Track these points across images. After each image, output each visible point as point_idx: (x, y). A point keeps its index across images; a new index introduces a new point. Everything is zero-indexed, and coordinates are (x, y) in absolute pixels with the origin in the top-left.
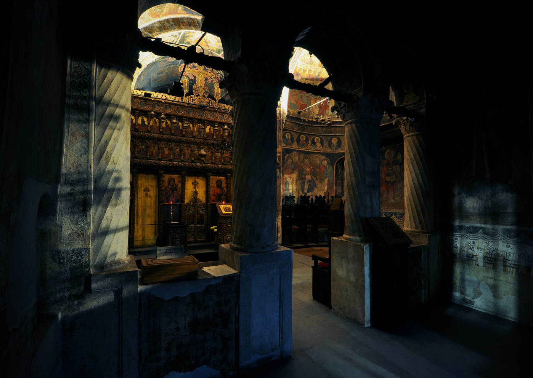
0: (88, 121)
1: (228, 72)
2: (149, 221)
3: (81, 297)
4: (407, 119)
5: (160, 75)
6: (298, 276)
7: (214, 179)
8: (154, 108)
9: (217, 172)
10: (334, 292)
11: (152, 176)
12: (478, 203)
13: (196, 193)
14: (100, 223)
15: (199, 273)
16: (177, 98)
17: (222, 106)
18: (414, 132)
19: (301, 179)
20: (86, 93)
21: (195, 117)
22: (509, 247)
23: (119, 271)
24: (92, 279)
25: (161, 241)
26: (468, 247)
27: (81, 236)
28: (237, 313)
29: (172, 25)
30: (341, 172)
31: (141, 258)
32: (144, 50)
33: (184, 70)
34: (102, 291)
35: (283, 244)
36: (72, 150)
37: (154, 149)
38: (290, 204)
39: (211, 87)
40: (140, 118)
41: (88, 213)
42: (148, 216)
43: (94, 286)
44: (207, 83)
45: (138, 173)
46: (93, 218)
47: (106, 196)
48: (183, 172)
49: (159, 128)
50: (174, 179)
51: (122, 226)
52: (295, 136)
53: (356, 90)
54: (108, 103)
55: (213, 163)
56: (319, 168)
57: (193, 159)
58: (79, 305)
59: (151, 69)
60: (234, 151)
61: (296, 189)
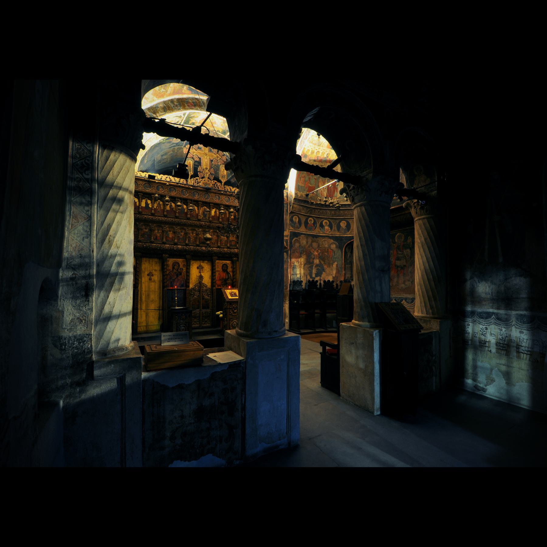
1: (234, 154)
2: (153, 306)
4: (418, 202)
5: (165, 157)
6: (306, 362)
7: (219, 263)
10: (343, 379)
11: (156, 260)
12: (491, 288)
13: (201, 277)
15: (204, 359)
16: (182, 180)
17: (228, 188)
18: (425, 215)
19: (309, 263)
22: (523, 333)
25: (165, 327)
26: (481, 333)
27: (84, 321)
28: (243, 402)
29: (177, 106)
30: (350, 256)
31: (145, 344)
32: (148, 131)
33: (188, 152)
35: (291, 330)
39: (217, 169)
40: (144, 201)
42: (152, 301)
44: (213, 164)
49: (164, 211)
52: (303, 220)
53: (365, 172)
55: (219, 247)
56: (328, 252)
57: (198, 243)
59: (155, 151)
60: (240, 235)
61: (304, 274)
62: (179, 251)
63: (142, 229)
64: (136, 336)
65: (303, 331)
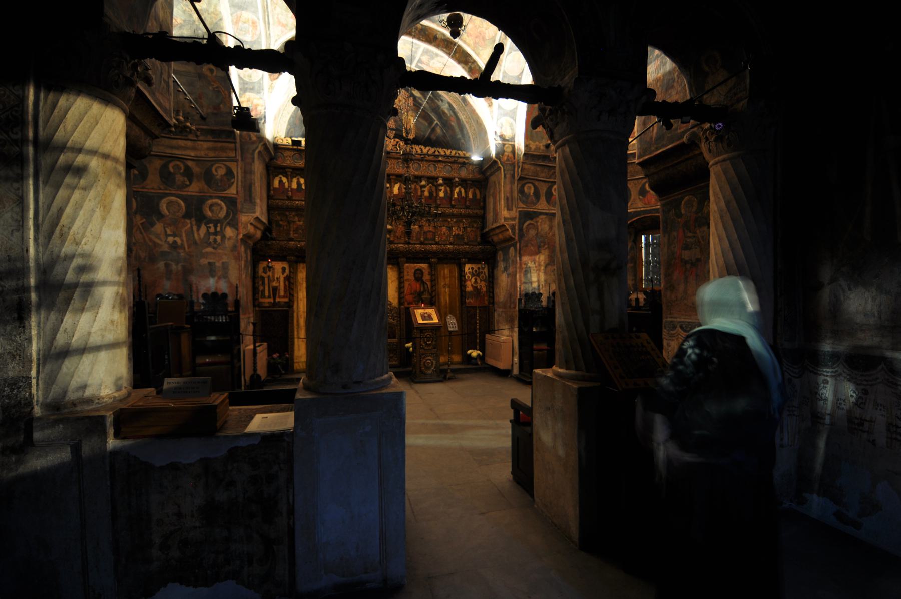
0: (21, 178)
9: (415, 257)
14: (53, 338)
20: (16, 134)
24: (34, 424)
34: (49, 445)
38: (532, 306)
41: (26, 322)
43: (37, 435)
45: (297, 262)
47: (62, 295)
61: (546, 281)
63: (294, 222)
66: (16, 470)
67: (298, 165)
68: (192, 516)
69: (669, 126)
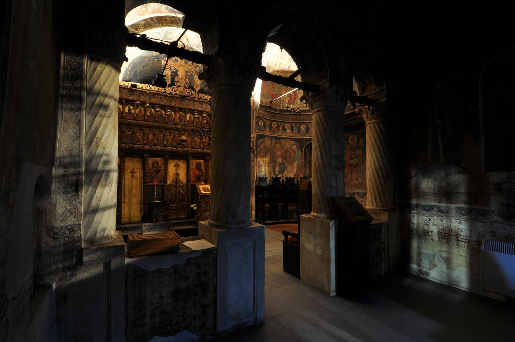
0: (80, 110)
2: (135, 200)
3: (73, 269)
8: (140, 97)
9: (197, 156)
11: (138, 159)
14: (90, 201)
16: (161, 89)
19: (273, 162)
20: (78, 84)
21: (176, 106)
23: (108, 245)
24: (84, 252)
25: (146, 218)
33: (166, 64)
34: (92, 263)
35: (257, 221)
36: (65, 136)
37: (139, 135)
38: (263, 184)
39: (192, 79)
41: (80, 193)
42: (135, 195)
43: (85, 259)
45: (125, 157)
46: (85, 197)
47: (96, 177)
48: (166, 156)
50: (158, 162)
51: (111, 204)
54: (98, 94)
56: (289, 152)
57: (175, 144)
58: (72, 275)
61: (269, 171)
62: (157, 151)
63: (125, 132)
64: (120, 227)
65: (267, 222)
66: (70, 280)
67: (130, 98)
68: (168, 297)
69: (354, 106)
